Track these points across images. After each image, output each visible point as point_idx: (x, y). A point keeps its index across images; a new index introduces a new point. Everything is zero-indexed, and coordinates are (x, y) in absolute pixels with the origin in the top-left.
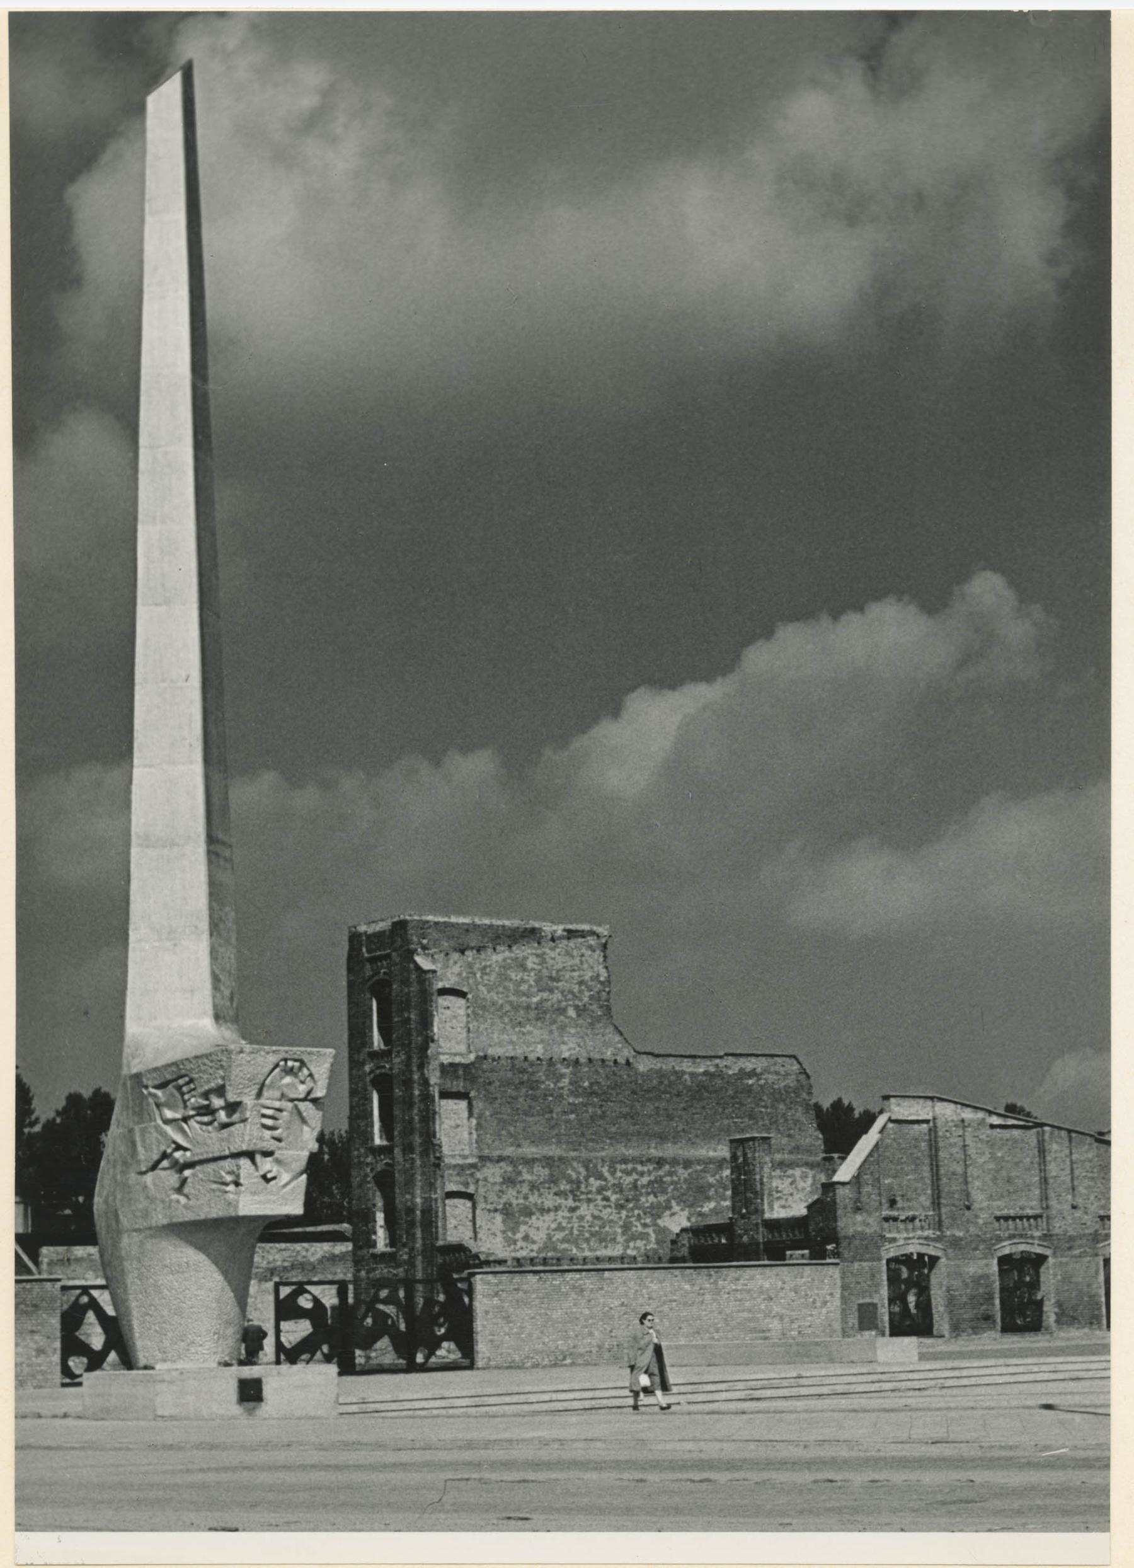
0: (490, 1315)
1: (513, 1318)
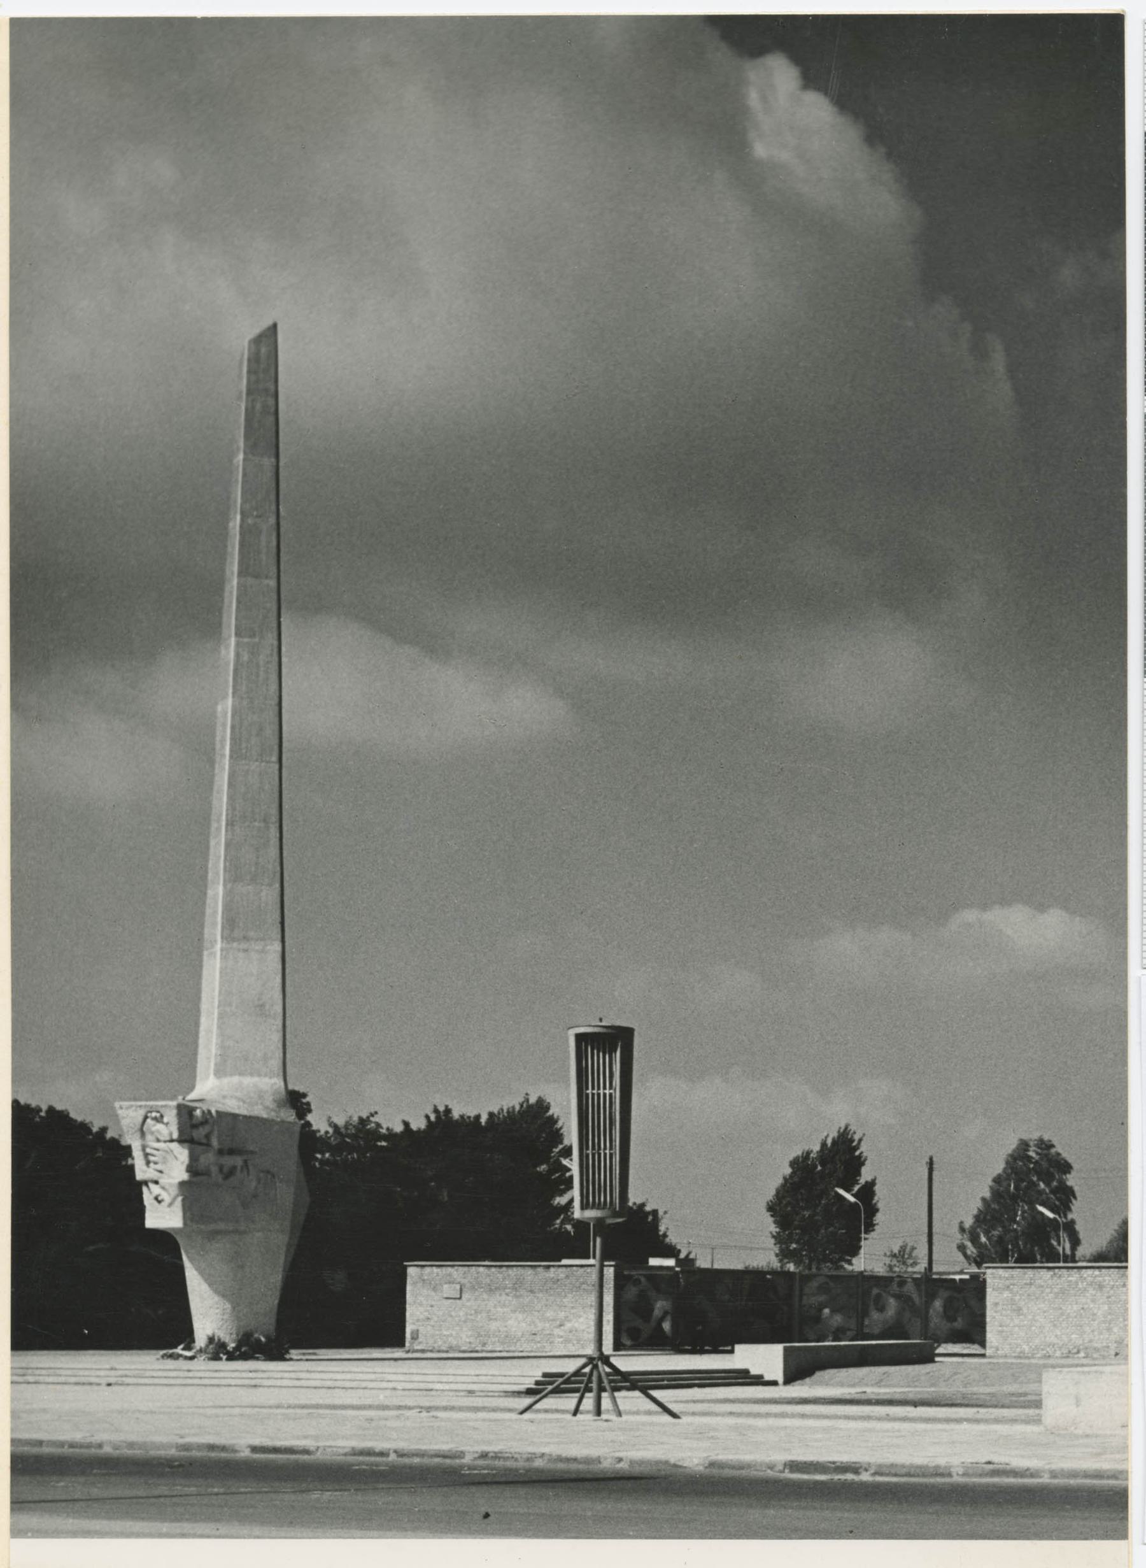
0: (1000, 1308)
1: (1025, 1311)
